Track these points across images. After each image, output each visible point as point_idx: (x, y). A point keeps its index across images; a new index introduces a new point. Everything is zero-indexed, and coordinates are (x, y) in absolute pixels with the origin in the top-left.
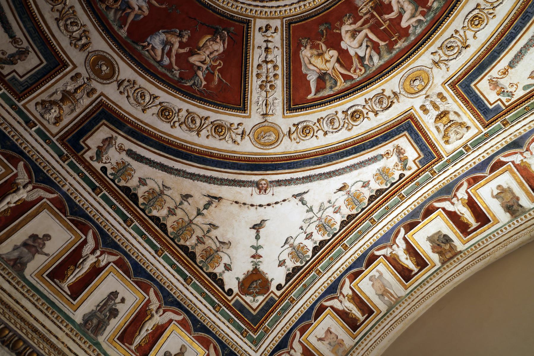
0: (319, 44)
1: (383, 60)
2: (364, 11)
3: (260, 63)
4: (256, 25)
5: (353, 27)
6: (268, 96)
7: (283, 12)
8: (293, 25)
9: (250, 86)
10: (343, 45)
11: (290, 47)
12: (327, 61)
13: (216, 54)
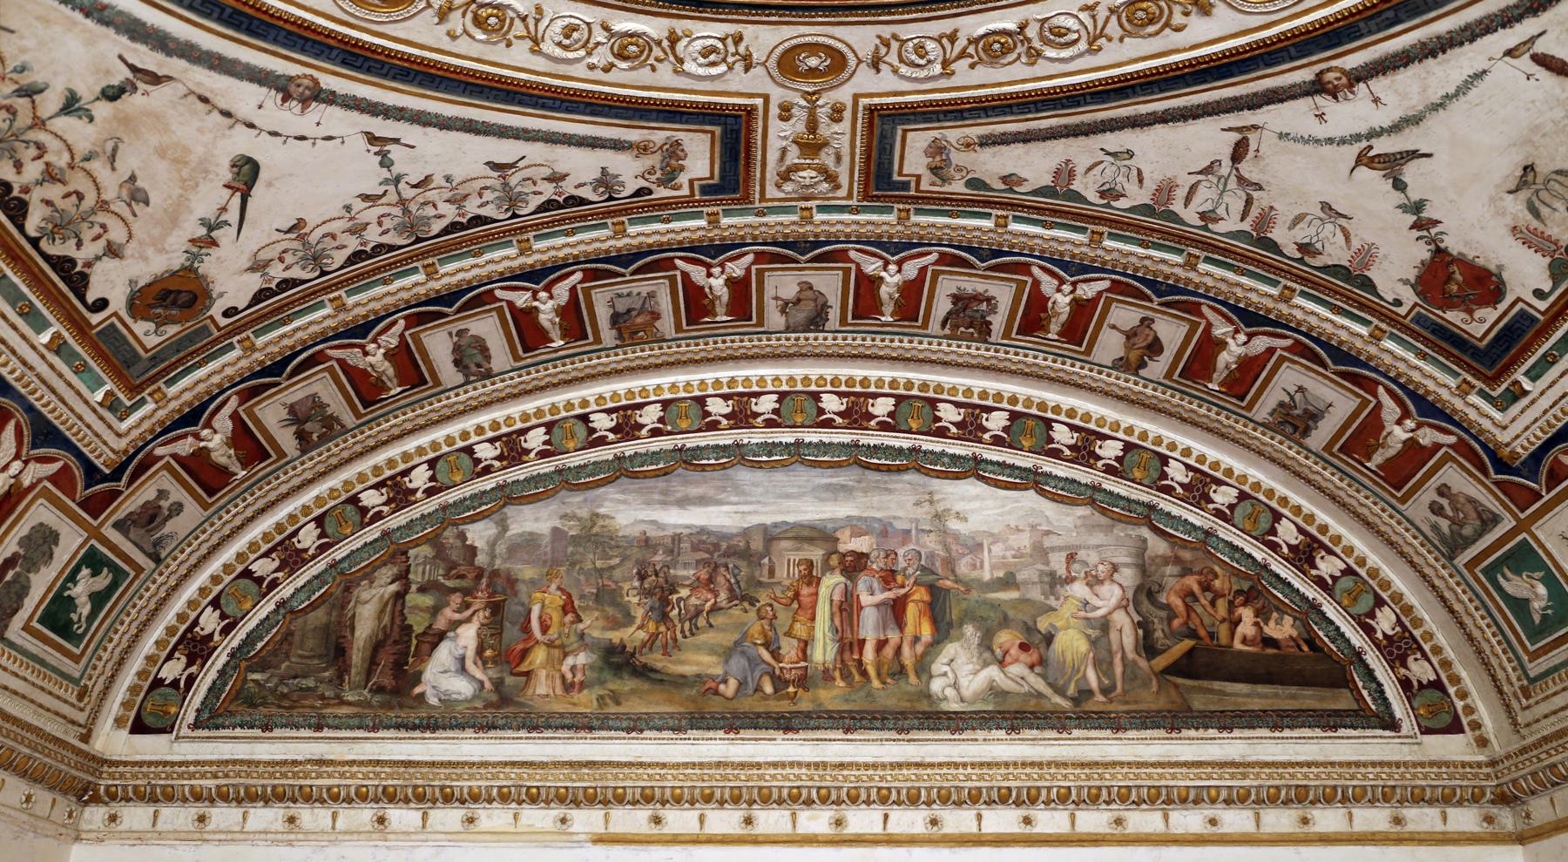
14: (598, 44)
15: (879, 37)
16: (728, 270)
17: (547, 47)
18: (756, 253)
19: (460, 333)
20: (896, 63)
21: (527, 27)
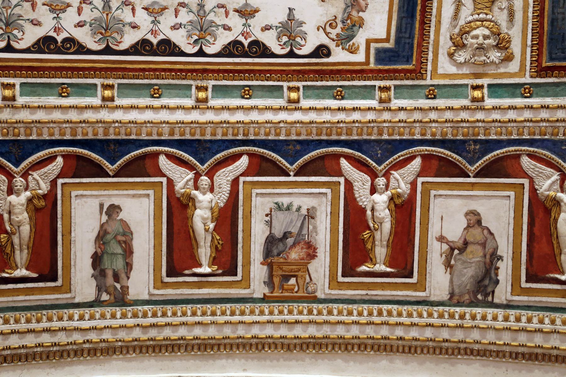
16: (393, 183)
18: (426, 158)
19: (114, 210)
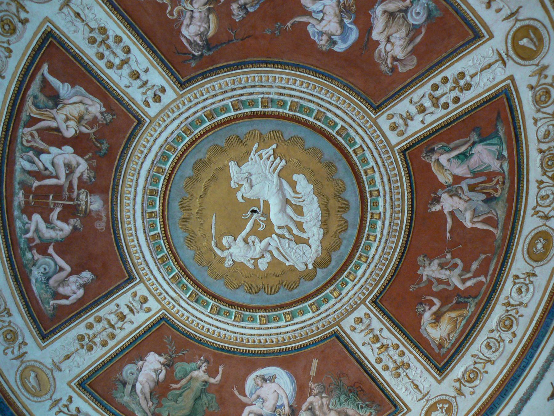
0: (92, 128)
1: (19, 170)
2: (83, 197)
3: (130, 55)
4: (172, 91)
5: (77, 174)
6: (86, 27)
7: (157, 128)
8: (135, 124)
9: (116, 19)
10: (68, 149)
11: (117, 99)
12: (67, 119)
13: (186, 21)
14: (500, 336)
15: (532, 216)
17: (493, 357)
20: (550, 208)
21: (480, 363)
